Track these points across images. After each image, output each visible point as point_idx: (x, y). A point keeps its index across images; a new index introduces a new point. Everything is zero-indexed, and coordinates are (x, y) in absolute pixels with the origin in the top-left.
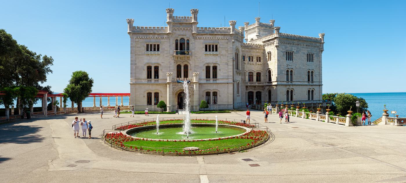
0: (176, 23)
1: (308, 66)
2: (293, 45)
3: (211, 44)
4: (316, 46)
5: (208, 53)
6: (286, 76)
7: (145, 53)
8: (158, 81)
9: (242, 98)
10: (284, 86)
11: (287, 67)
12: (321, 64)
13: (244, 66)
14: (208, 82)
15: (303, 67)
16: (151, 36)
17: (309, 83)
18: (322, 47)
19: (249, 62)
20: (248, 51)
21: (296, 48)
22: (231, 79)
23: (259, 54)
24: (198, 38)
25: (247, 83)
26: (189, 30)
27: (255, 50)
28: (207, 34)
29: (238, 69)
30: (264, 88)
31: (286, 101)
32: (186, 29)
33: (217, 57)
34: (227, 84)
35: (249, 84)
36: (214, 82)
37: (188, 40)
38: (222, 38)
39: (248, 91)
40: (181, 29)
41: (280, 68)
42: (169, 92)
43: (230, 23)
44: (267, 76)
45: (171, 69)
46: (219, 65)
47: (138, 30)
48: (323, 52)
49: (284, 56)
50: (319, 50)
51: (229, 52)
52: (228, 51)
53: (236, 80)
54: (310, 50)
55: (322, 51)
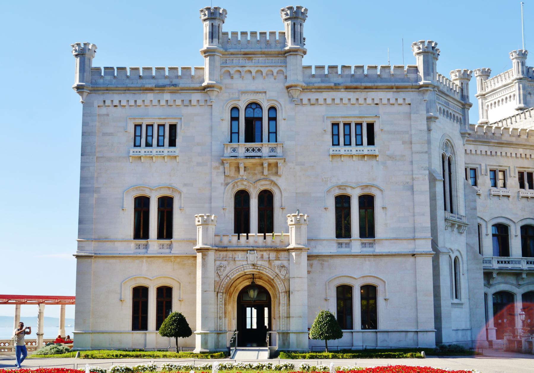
0: (232, 54)
3: (353, 121)
5: (342, 152)
7: (129, 152)
8: (170, 246)
9: (472, 315)
13: (475, 201)
14: (344, 250)
16: (150, 96)
19: (494, 189)
20: (489, 153)
22: (425, 238)
24: (305, 101)
25: (490, 262)
26: (275, 74)
27: (510, 150)
28: (336, 87)
29: (452, 212)
32: (265, 70)
33: (373, 162)
34: (412, 259)
35: (496, 265)
36: (365, 249)
37: (272, 109)
38: (389, 100)
39: (492, 291)
40: (250, 72)
42: (203, 283)
43: (416, 50)
45: (213, 205)
46: (381, 190)
47: (108, 78)
51: (416, 147)
52: (411, 143)
53: (444, 247)
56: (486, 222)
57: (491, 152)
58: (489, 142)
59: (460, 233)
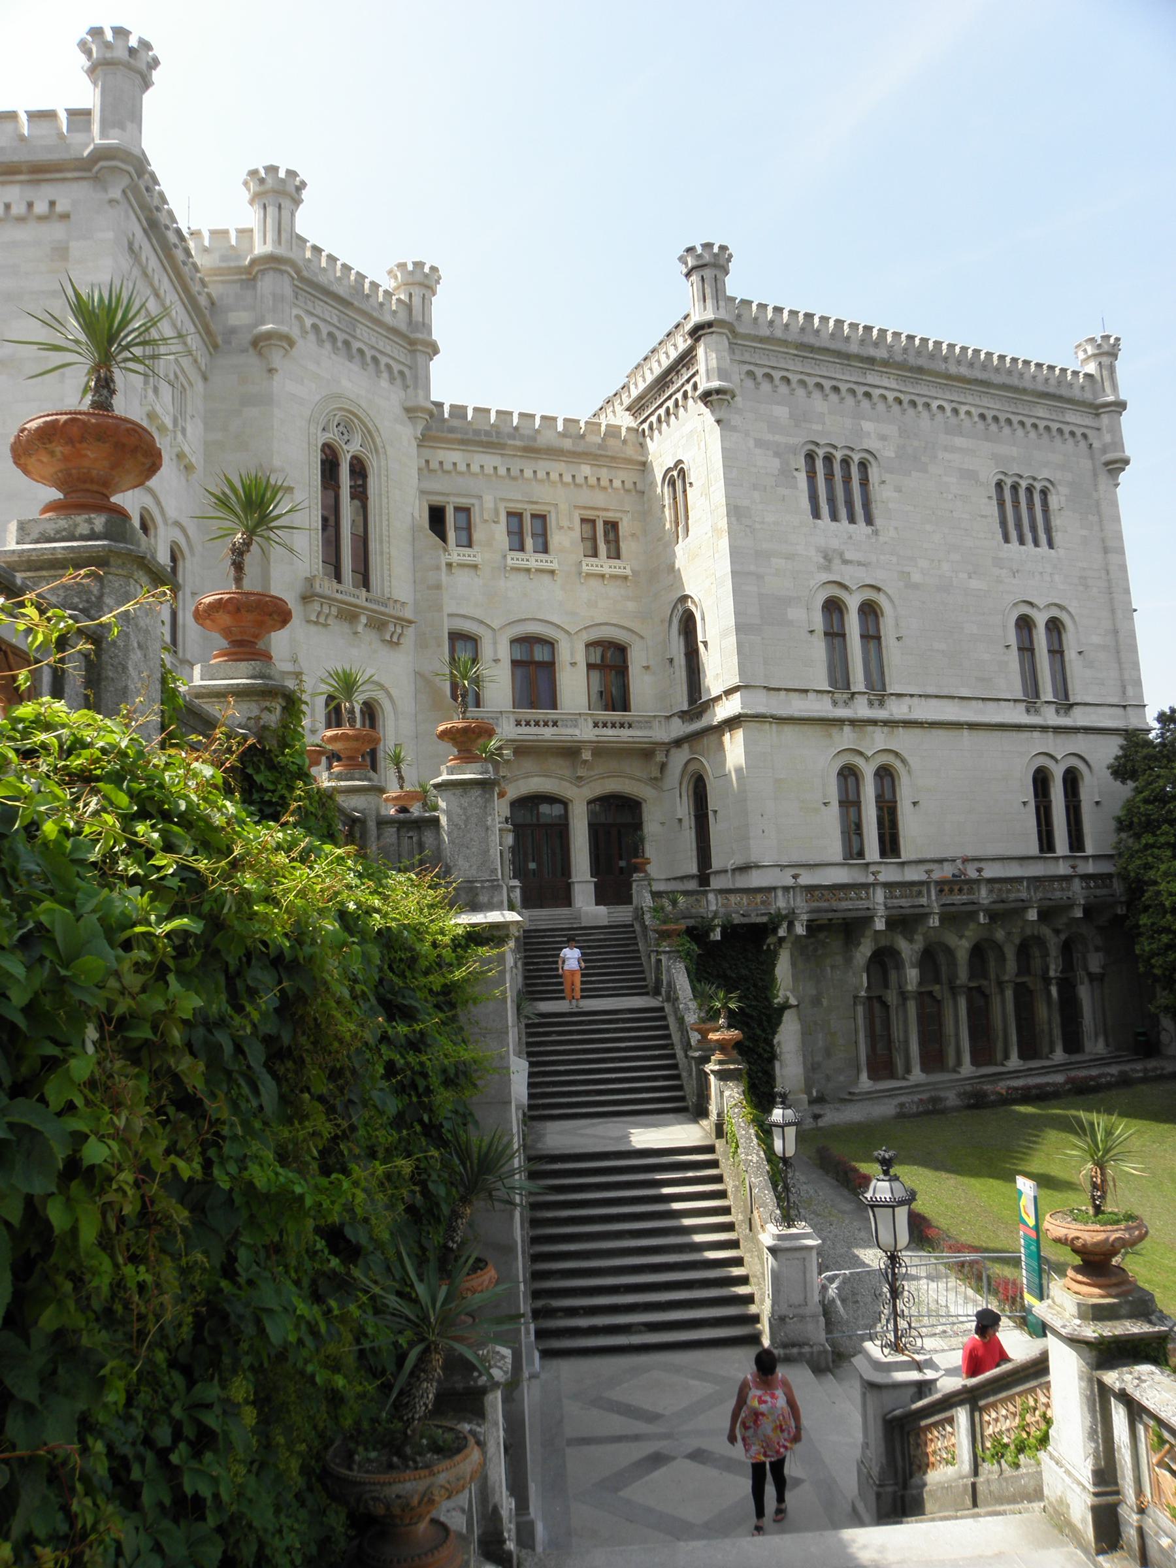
1: (1014, 574)
2: (865, 403)
4: (1060, 431)
6: (818, 649)
10: (807, 729)
11: (825, 577)
12: (1123, 568)
15: (974, 584)
17: (1037, 712)
18: (1108, 438)
21: (891, 430)
23: (599, 499)
27: (556, 468)
30: (663, 767)
31: (839, 858)
41: (760, 577)
44: (671, 660)
48: (1122, 477)
49: (795, 487)
50: (1092, 458)
54: (1014, 451)
55: (1117, 465)
56: (493, 630)
57: (508, 470)
58: (503, 446)
59: (391, 642)
